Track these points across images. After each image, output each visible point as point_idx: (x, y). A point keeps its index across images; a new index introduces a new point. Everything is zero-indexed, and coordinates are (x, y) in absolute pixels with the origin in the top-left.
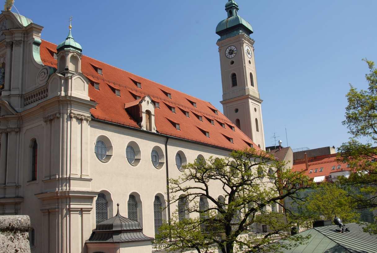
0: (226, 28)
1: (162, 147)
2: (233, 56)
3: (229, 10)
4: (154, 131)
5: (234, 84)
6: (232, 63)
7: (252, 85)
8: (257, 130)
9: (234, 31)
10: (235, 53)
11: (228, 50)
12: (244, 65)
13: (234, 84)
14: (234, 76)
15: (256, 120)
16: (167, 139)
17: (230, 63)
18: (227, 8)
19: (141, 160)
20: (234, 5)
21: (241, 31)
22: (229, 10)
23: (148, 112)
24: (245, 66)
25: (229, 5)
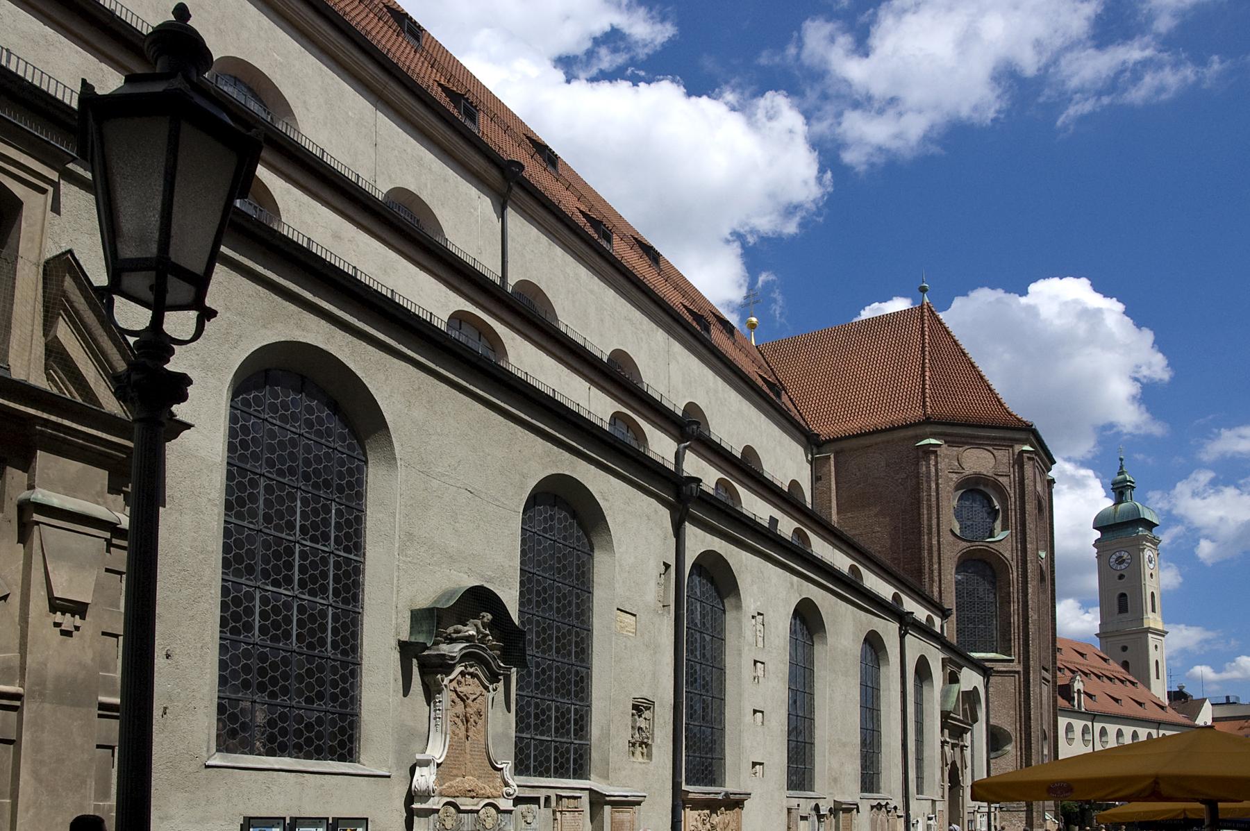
0: (1113, 523)
1: (1090, 724)
2: (1123, 567)
3: (1118, 491)
4: (1083, 710)
5: (1123, 608)
6: (1121, 577)
7: (1154, 610)
8: (1158, 678)
9: (1128, 527)
10: (1127, 563)
11: (1114, 556)
12: (1143, 582)
13: (1123, 608)
14: (1123, 596)
15: (1157, 662)
16: (1094, 717)
17: (1116, 578)
18: (1115, 487)
19: (1075, 740)
20: (1129, 484)
21: (1140, 529)
22: (1118, 491)
23: (1079, 690)
24: (1145, 584)
25: (1120, 482)
